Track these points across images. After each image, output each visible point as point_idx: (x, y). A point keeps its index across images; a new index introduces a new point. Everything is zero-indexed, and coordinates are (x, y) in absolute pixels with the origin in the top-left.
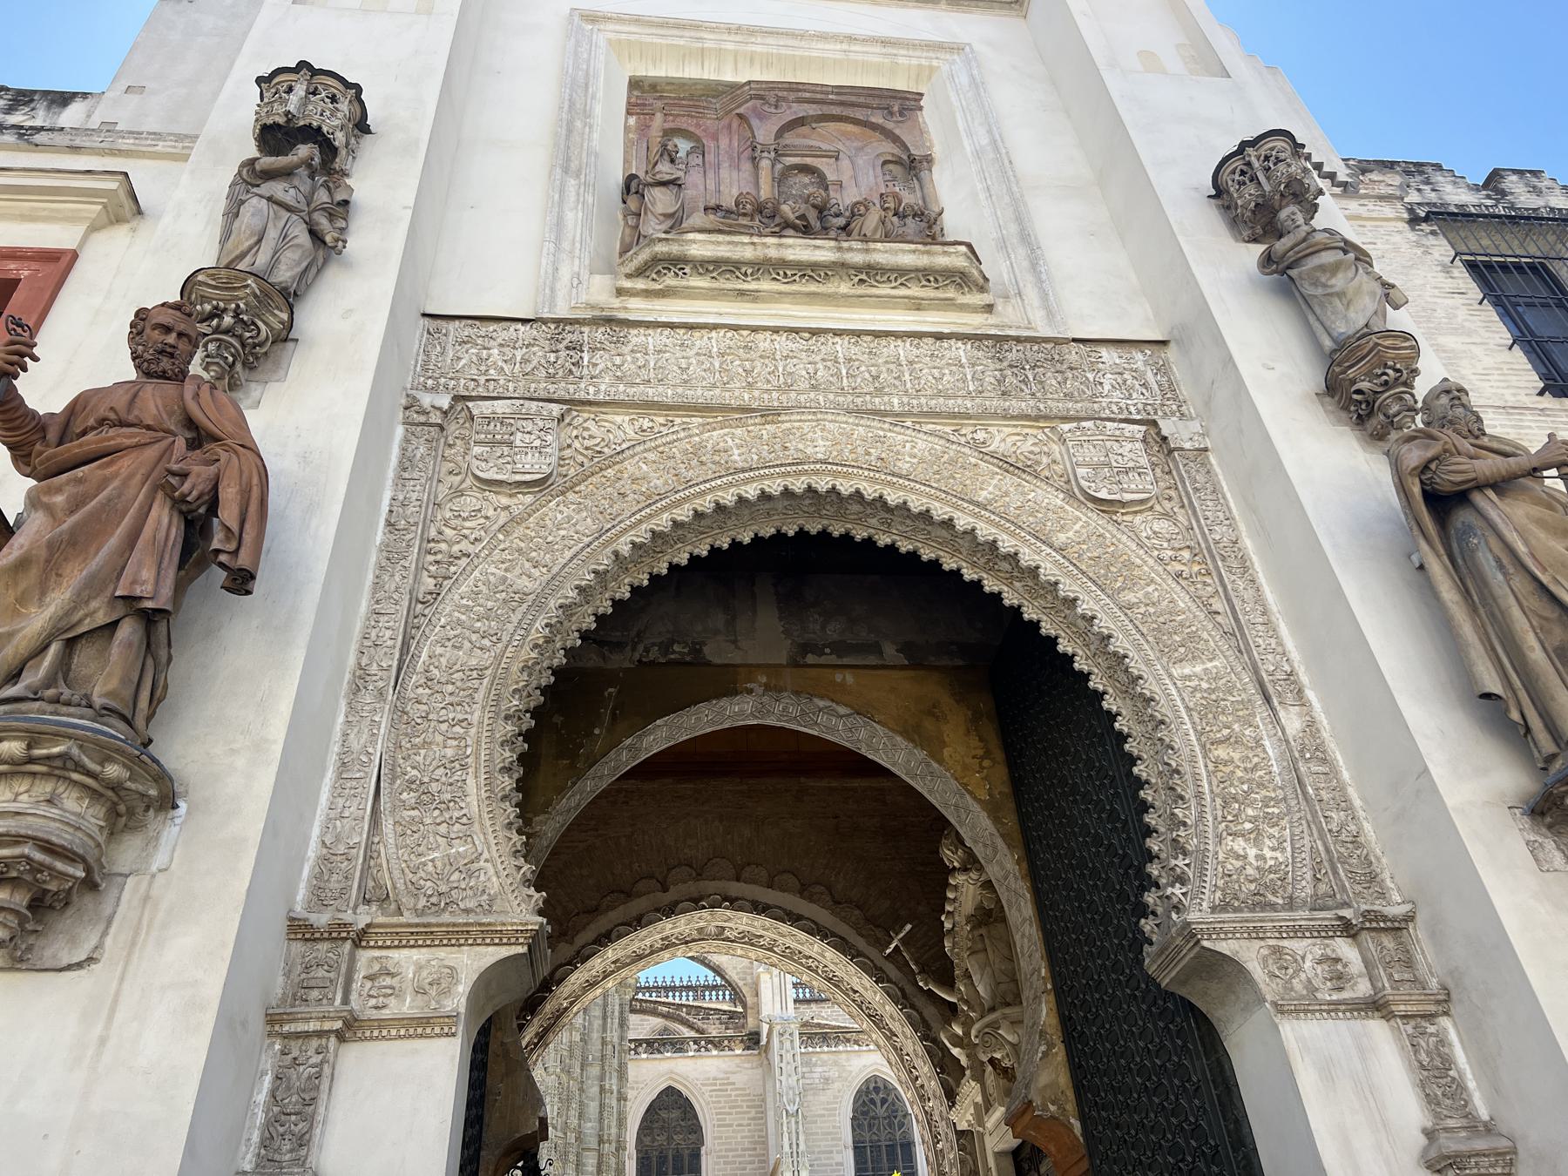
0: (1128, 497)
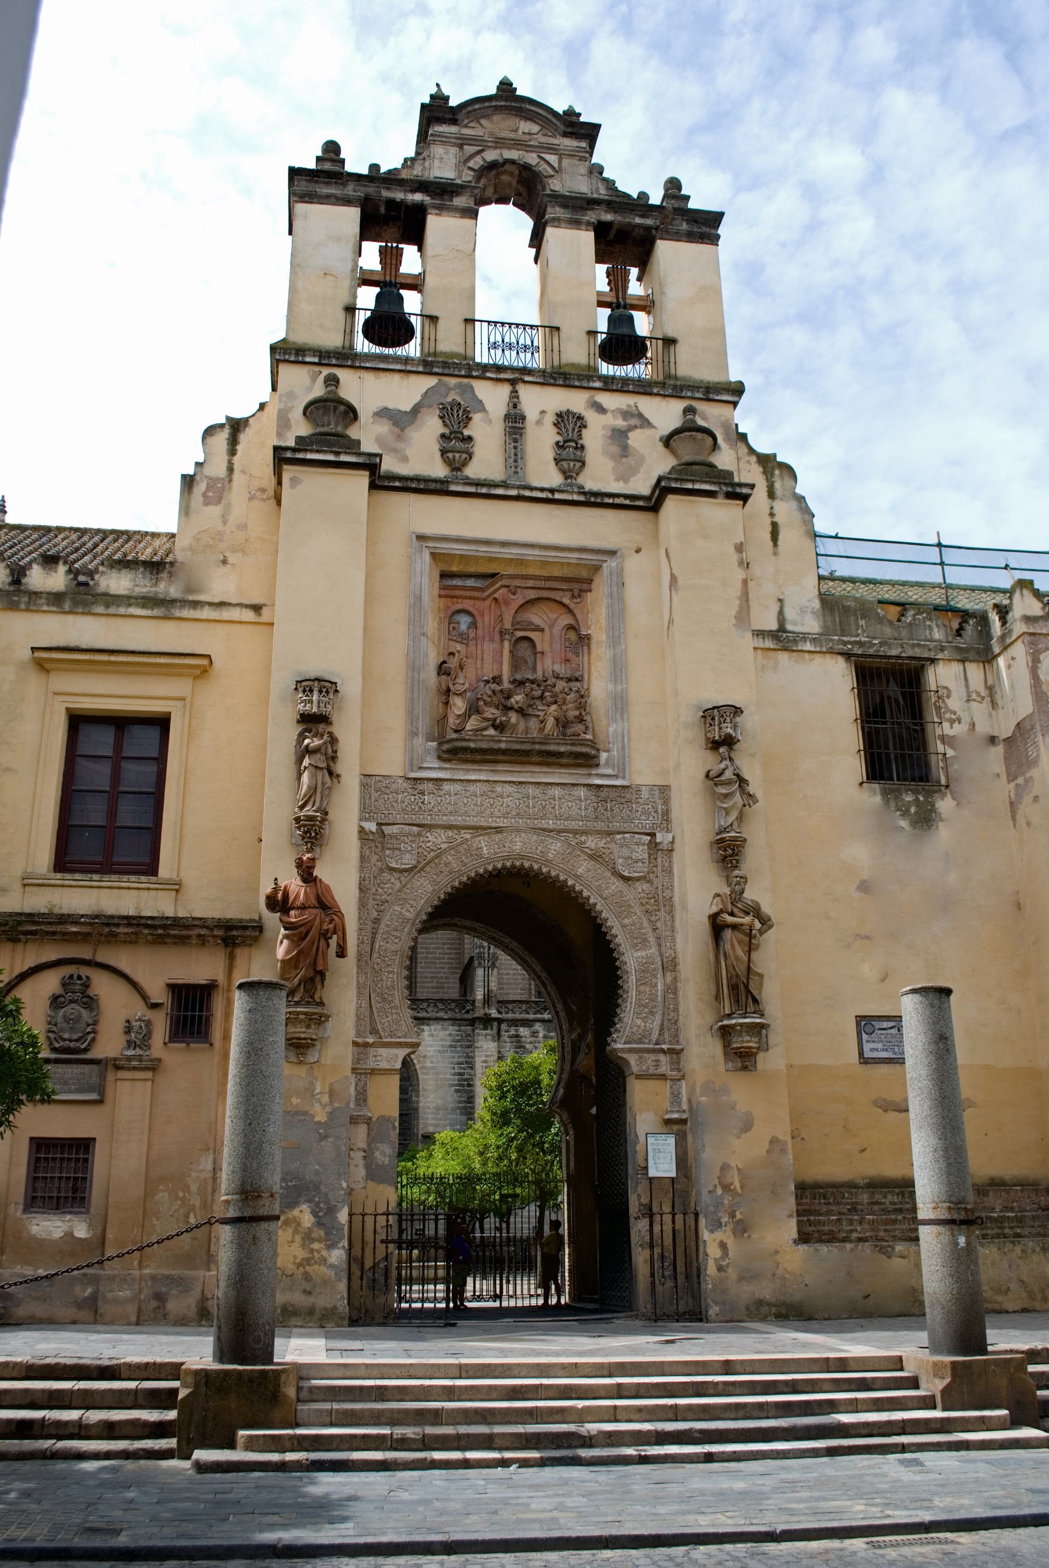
0: (636, 875)
